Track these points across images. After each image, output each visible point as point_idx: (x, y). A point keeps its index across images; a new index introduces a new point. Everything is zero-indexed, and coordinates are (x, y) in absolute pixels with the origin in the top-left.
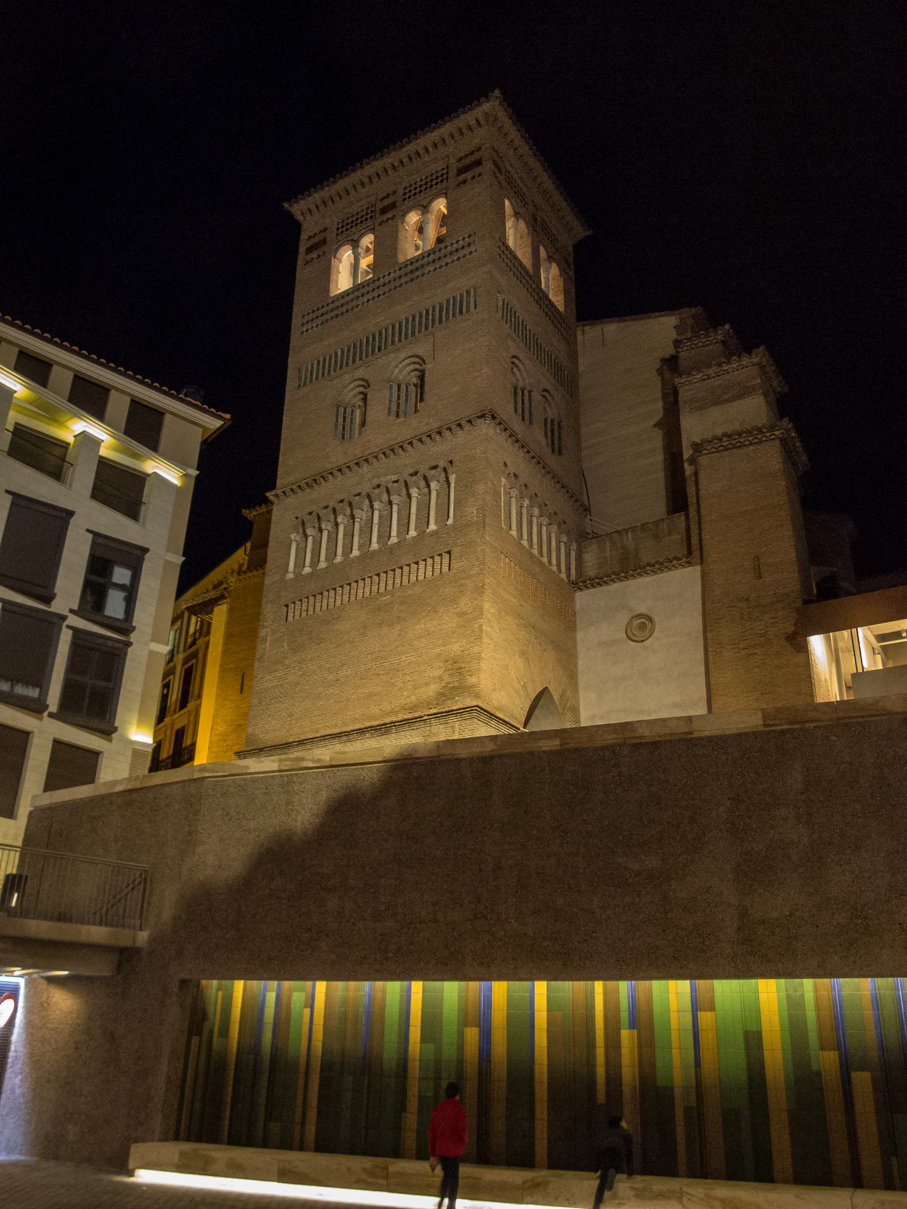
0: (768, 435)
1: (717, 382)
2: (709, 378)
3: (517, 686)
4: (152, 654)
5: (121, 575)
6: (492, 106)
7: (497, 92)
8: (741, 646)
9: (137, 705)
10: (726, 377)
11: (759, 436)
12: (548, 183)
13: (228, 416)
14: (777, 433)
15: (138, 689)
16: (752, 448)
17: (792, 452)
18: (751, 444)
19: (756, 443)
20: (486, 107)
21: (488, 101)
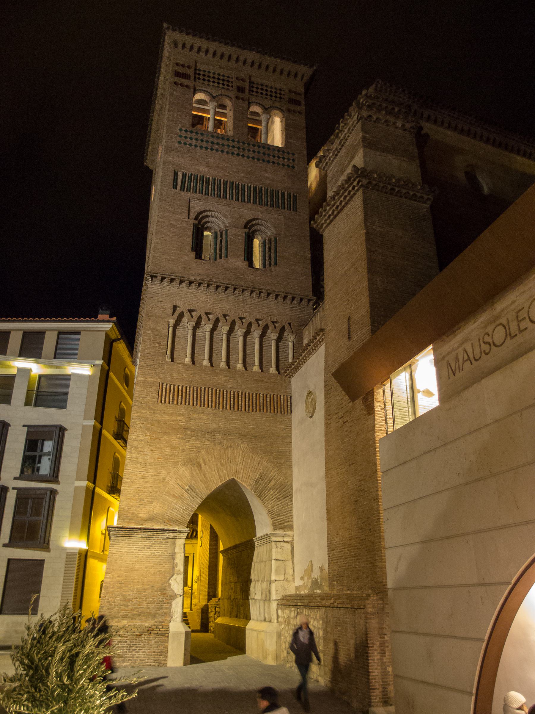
0: (350, 189)
1: (343, 152)
2: (339, 152)
3: (178, 491)
4: (77, 488)
5: (48, 446)
6: (170, 37)
7: (165, 25)
8: (340, 415)
9: (68, 524)
10: (347, 143)
11: (346, 194)
12: (251, 56)
13: (114, 318)
14: (355, 183)
15: (69, 513)
16: (349, 206)
17: (393, 189)
18: (346, 204)
19: (349, 200)
20: (167, 39)
21: (165, 34)
